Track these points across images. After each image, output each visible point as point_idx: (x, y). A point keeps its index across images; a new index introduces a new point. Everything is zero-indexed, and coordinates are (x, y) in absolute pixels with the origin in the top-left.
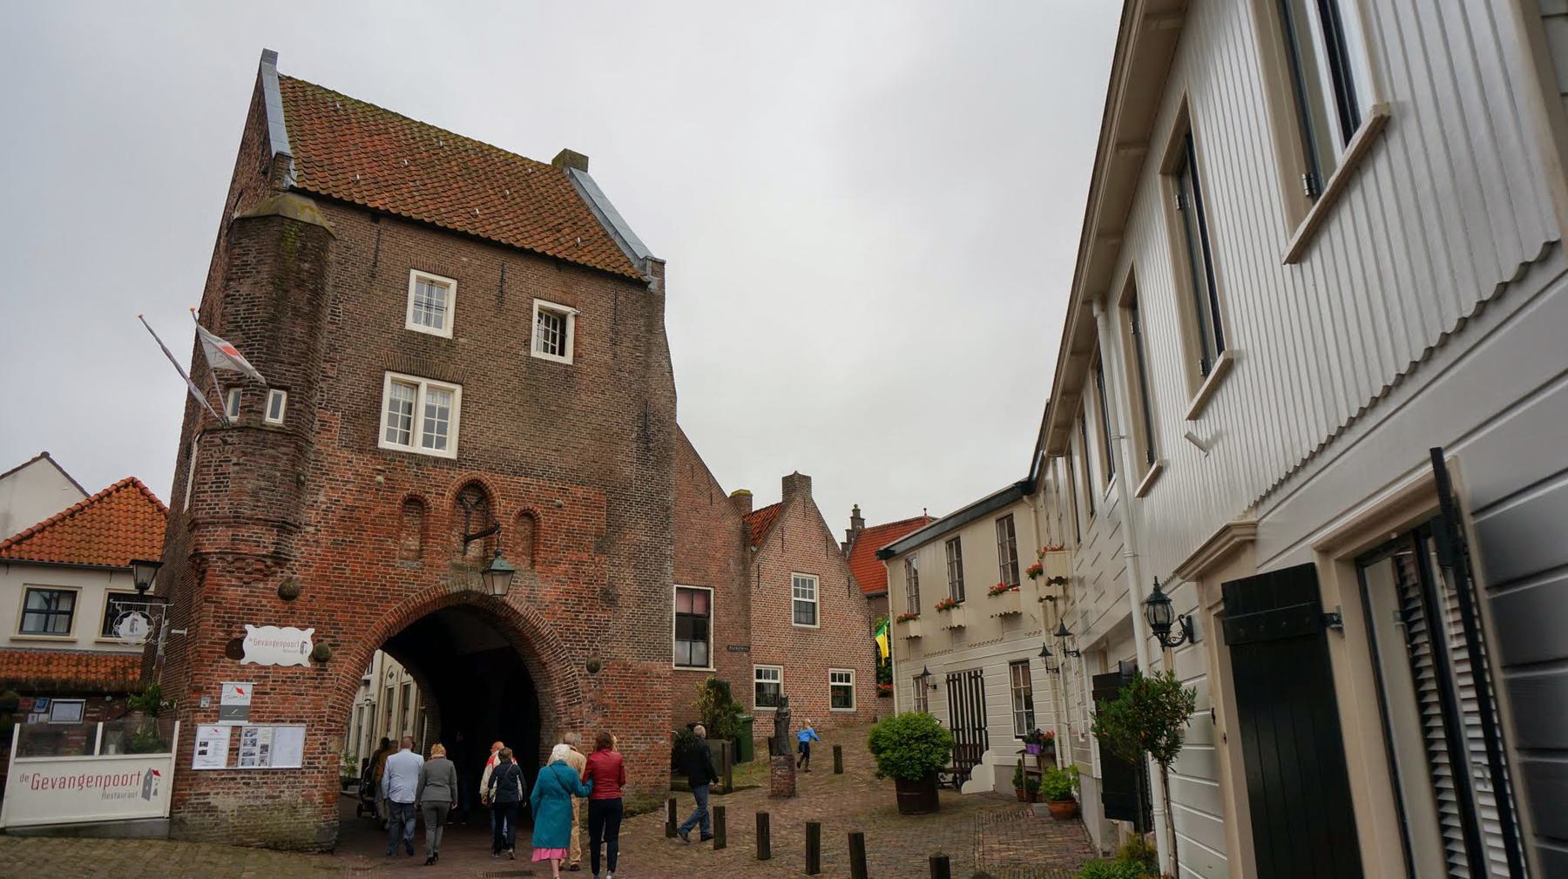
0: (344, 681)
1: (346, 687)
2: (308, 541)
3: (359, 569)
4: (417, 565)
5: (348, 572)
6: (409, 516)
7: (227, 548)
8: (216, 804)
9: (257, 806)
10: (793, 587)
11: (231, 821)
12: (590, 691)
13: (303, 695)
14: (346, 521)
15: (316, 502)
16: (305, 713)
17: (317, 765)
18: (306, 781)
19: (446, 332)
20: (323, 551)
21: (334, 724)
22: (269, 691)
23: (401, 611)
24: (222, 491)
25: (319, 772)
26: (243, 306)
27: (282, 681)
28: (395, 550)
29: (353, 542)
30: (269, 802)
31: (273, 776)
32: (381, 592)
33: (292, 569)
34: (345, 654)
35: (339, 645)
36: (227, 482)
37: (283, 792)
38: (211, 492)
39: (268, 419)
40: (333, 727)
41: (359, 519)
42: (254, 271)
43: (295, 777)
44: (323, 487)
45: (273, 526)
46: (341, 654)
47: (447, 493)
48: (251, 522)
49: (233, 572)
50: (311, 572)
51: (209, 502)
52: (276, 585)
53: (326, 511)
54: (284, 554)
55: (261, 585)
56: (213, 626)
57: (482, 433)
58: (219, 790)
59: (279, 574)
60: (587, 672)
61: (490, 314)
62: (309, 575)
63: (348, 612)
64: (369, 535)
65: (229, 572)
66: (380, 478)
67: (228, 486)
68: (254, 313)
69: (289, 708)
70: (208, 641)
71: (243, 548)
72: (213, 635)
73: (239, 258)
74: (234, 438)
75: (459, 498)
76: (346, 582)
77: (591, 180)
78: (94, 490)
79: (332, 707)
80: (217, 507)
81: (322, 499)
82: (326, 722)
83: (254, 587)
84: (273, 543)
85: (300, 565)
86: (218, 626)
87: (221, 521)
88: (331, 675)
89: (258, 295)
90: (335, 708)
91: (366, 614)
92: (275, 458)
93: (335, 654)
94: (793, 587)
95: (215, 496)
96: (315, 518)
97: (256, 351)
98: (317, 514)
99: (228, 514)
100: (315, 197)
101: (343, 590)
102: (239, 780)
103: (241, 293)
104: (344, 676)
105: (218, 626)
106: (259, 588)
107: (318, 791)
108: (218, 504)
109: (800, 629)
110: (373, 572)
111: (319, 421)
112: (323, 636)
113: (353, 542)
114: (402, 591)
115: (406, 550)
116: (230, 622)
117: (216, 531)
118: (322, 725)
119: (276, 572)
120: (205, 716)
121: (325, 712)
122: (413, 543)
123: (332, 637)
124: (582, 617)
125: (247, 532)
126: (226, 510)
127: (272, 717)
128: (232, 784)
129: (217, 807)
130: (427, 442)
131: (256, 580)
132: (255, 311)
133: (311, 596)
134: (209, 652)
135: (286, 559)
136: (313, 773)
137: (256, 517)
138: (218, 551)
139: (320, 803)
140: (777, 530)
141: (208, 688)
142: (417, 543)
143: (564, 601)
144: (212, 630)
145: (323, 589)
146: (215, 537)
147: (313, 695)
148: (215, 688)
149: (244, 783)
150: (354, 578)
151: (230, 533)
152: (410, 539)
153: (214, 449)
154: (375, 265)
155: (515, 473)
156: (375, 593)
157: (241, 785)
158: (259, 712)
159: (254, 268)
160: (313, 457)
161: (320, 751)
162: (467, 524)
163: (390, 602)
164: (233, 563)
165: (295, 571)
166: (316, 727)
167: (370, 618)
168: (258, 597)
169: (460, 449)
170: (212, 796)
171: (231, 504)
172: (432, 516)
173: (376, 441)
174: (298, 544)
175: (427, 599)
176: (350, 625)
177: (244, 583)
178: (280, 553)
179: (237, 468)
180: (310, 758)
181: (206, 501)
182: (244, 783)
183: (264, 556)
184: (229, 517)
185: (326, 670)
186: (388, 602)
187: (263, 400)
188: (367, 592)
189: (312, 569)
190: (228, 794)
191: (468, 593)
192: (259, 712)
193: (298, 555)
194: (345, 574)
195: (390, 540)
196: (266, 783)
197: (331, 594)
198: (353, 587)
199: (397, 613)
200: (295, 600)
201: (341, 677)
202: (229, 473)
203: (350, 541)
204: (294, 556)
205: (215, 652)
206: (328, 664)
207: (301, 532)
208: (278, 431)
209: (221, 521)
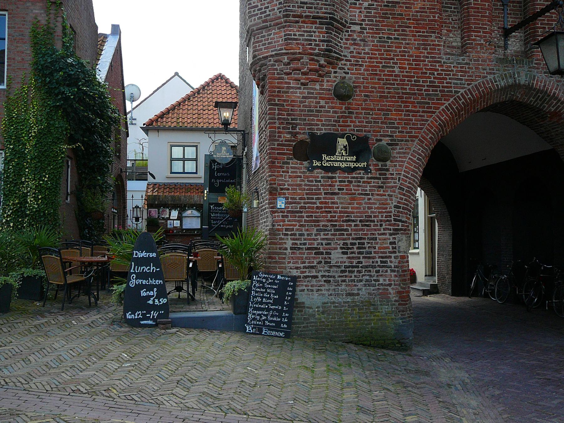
0: (406, 181)
1: (408, 187)
2: (355, 40)
3: (407, 67)
4: (463, 60)
5: (397, 70)
6: (447, 11)
7: (281, 49)
8: (303, 300)
9: (340, 303)
11: (317, 316)
13: (368, 195)
14: (389, 18)
16: (372, 212)
17: (389, 264)
18: (381, 279)
20: (372, 50)
21: (400, 223)
22: (337, 191)
23: (452, 108)
25: (392, 271)
27: (348, 181)
28: (439, 45)
29: (398, 39)
31: (350, 274)
32: (431, 89)
33: (343, 69)
34: (404, 153)
35: (397, 145)
40: (400, 227)
41: (402, 15)
43: (370, 276)
45: (321, 23)
46: (399, 153)
48: (301, 20)
49: (290, 74)
50: (362, 71)
52: (331, 85)
53: (369, 8)
54: (335, 52)
55: (318, 87)
56: (279, 128)
58: (304, 288)
59: (333, 75)
62: (360, 74)
63: (402, 111)
64: (413, 31)
69: (357, 208)
70: (276, 143)
72: (280, 137)
76: (396, 80)
78: (197, 84)
79: (396, 207)
82: (393, 222)
83: (312, 89)
85: (351, 65)
86: (283, 128)
87: (272, 23)
88: (392, 174)
90: (399, 207)
91: (418, 112)
93: (394, 153)
96: (360, 16)
98: (360, 12)
99: (279, 15)
101: (395, 89)
102: (320, 278)
104: (404, 176)
105: (283, 128)
106: (315, 89)
107: (393, 289)
108: (267, 7)
110: (421, 69)
113: (398, 39)
114: (451, 87)
115: (448, 47)
116: (294, 123)
118: (390, 225)
120: (283, 216)
121: (391, 212)
122: (455, 40)
123: (390, 136)
125: (299, 31)
126: (276, 10)
127: (343, 217)
128: (314, 282)
129: (303, 303)
131: (313, 81)
133: (365, 96)
134: (278, 154)
135: (338, 59)
136: (386, 271)
137: (304, 14)
138: (274, 53)
139: (396, 301)
141: (282, 189)
142: (459, 39)
144: (279, 132)
145: (375, 88)
146: (270, 41)
147: (378, 195)
148: (288, 189)
149: (325, 281)
150: (403, 76)
152: (451, 35)
156: (425, 91)
157: (323, 283)
158: (330, 212)
161: (391, 250)
163: (441, 100)
164: (289, 64)
165: (347, 71)
166: (384, 227)
167: (423, 116)
168: (316, 98)
172: (472, 8)
174: (346, 44)
176: (405, 124)
177: (302, 84)
178: (330, 51)
180: (382, 257)
182: (325, 281)
183: (318, 55)
184: (280, 18)
185: (388, 170)
186: (438, 99)
188: (418, 90)
189: (362, 68)
190: (312, 291)
191: (516, 86)
192: (330, 212)
194: (394, 71)
195: (433, 35)
196: (344, 281)
197: (384, 92)
198: (403, 85)
199: (449, 110)
200: (351, 101)
201: (402, 177)
203: (395, 38)
204: (345, 56)
206: (388, 163)
207: (347, 31)
209: (272, 23)
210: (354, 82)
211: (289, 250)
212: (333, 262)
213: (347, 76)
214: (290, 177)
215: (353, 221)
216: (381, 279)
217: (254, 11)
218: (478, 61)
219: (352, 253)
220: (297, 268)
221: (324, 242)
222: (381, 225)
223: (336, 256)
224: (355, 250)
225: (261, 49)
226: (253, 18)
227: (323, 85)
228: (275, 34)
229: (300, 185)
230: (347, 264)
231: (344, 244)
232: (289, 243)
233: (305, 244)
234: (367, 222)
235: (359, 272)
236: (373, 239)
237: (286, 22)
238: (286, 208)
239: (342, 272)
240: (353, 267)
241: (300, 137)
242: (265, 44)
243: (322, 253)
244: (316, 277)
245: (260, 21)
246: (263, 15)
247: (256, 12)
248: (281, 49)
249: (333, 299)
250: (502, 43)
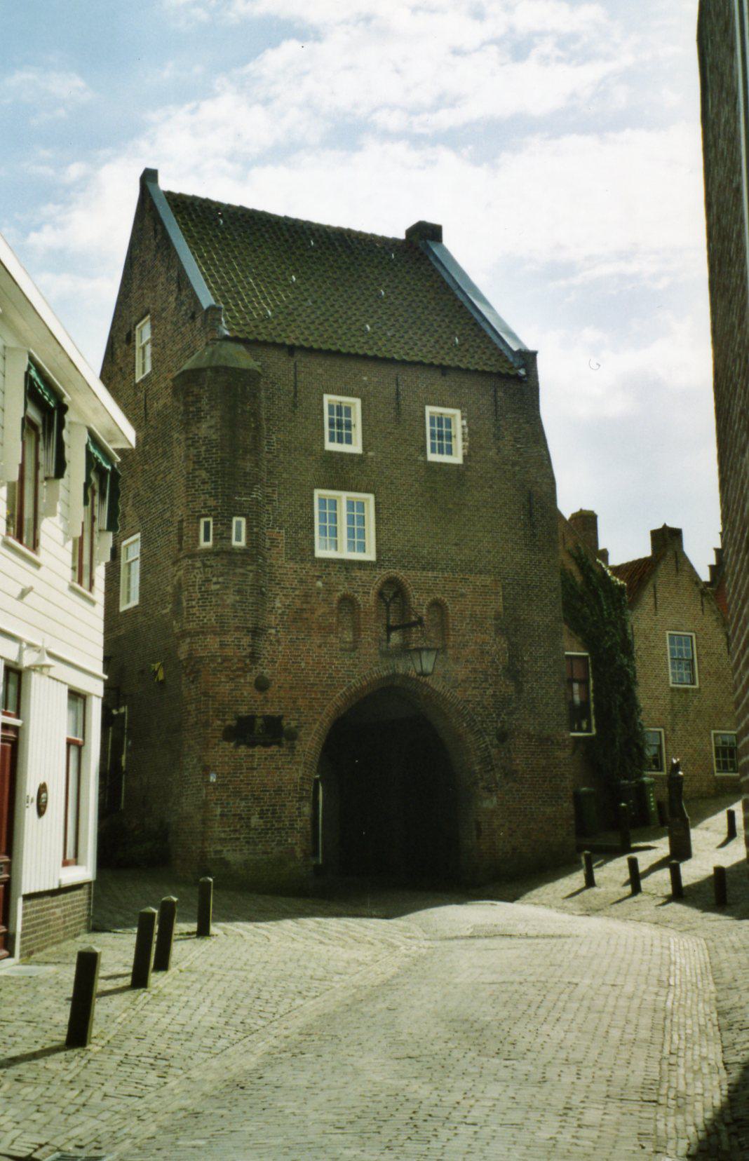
5: (303, 665)
10: (668, 647)
12: (501, 758)
15: (273, 608)
19: (356, 448)
30: (265, 857)
35: (302, 727)
37: (272, 849)
39: (235, 543)
44: (278, 594)
47: (371, 591)
57: (394, 535)
59: (254, 671)
60: (497, 742)
61: (392, 425)
65: (219, 671)
66: (319, 584)
68: (213, 454)
71: (229, 652)
74: (211, 561)
75: (380, 594)
77: (446, 251)
81: (278, 605)
84: (249, 646)
92: (243, 574)
93: (301, 734)
94: (668, 647)
100: (244, 342)
109: (678, 690)
111: (269, 539)
112: (291, 720)
119: (252, 669)
122: (348, 636)
124: (489, 692)
130: (351, 546)
140: (650, 587)
141: (214, 766)
143: (472, 679)
151: (218, 640)
154: (295, 396)
155: (424, 569)
160: (268, 571)
162: (388, 619)
164: (222, 663)
168: (240, 690)
169: (378, 552)
170: (225, 852)
173: (313, 551)
175: (365, 683)
179: (218, 587)
187: (230, 528)
190: (236, 850)
191: (395, 675)
193: (266, 654)
196: (260, 841)
205: (216, 737)
206: (296, 742)
208: (243, 552)
210: (271, 676)
211: (218, 818)
212: (253, 826)
213: (265, 671)
214: (220, 756)
215: (268, 791)
216: (290, 840)
218: (366, 655)
219: (267, 817)
220: (224, 832)
221: (246, 809)
222: (290, 794)
223: (255, 821)
224: (269, 815)
227: (245, 679)
229: (228, 763)
230: (263, 827)
231: (262, 810)
232: (218, 811)
233: (230, 811)
234: (279, 791)
235: (273, 833)
236: (282, 805)
238: (217, 781)
239: (259, 833)
240: (268, 829)
241: (228, 723)
243: (243, 819)
244: (238, 839)
246: (201, 623)
249: (251, 857)
250: (385, 637)
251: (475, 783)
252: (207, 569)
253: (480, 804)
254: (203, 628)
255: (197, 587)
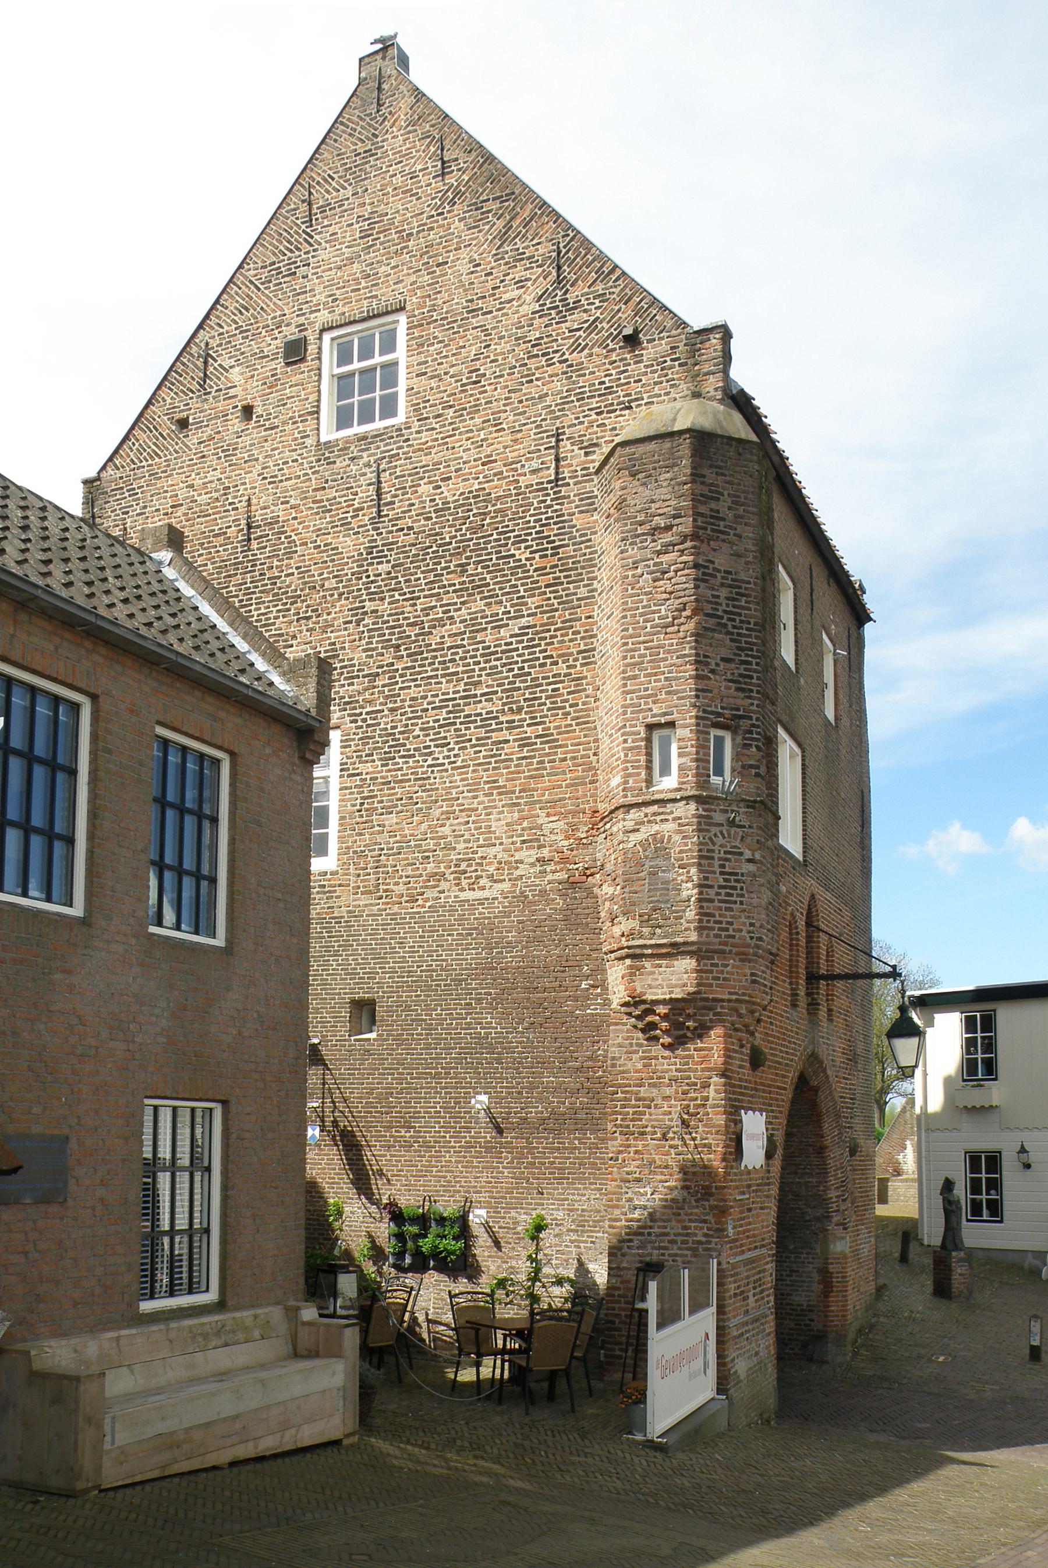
7: (744, 994)
24: (735, 902)
26: (723, 590)
36: (742, 889)
38: (720, 901)
42: (732, 532)
51: (718, 918)
67: (742, 896)
68: (743, 608)
73: (705, 503)
80: (731, 928)
87: (735, 950)
89: (743, 576)
95: (727, 909)
97: (755, 675)
103: (716, 565)
108: (731, 923)
117: (727, 966)
126: (744, 933)
132: (743, 603)
138: (734, 997)
151: (748, 971)
153: (714, 830)
159: (730, 527)
171: (752, 925)
179: (751, 867)
181: (713, 916)
184: (748, 946)
202: (742, 875)
209: (735, 950)
217: (708, 921)
225: (711, 985)
226: (705, 932)
228: (733, 967)
237: (755, 954)
242: (718, 979)
245: (717, 940)
246: (723, 934)
247: (711, 924)
248: (744, 994)
251: (828, 1218)
252: (733, 830)
253: (832, 1246)
254: (725, 944)
255: (717, 863)
